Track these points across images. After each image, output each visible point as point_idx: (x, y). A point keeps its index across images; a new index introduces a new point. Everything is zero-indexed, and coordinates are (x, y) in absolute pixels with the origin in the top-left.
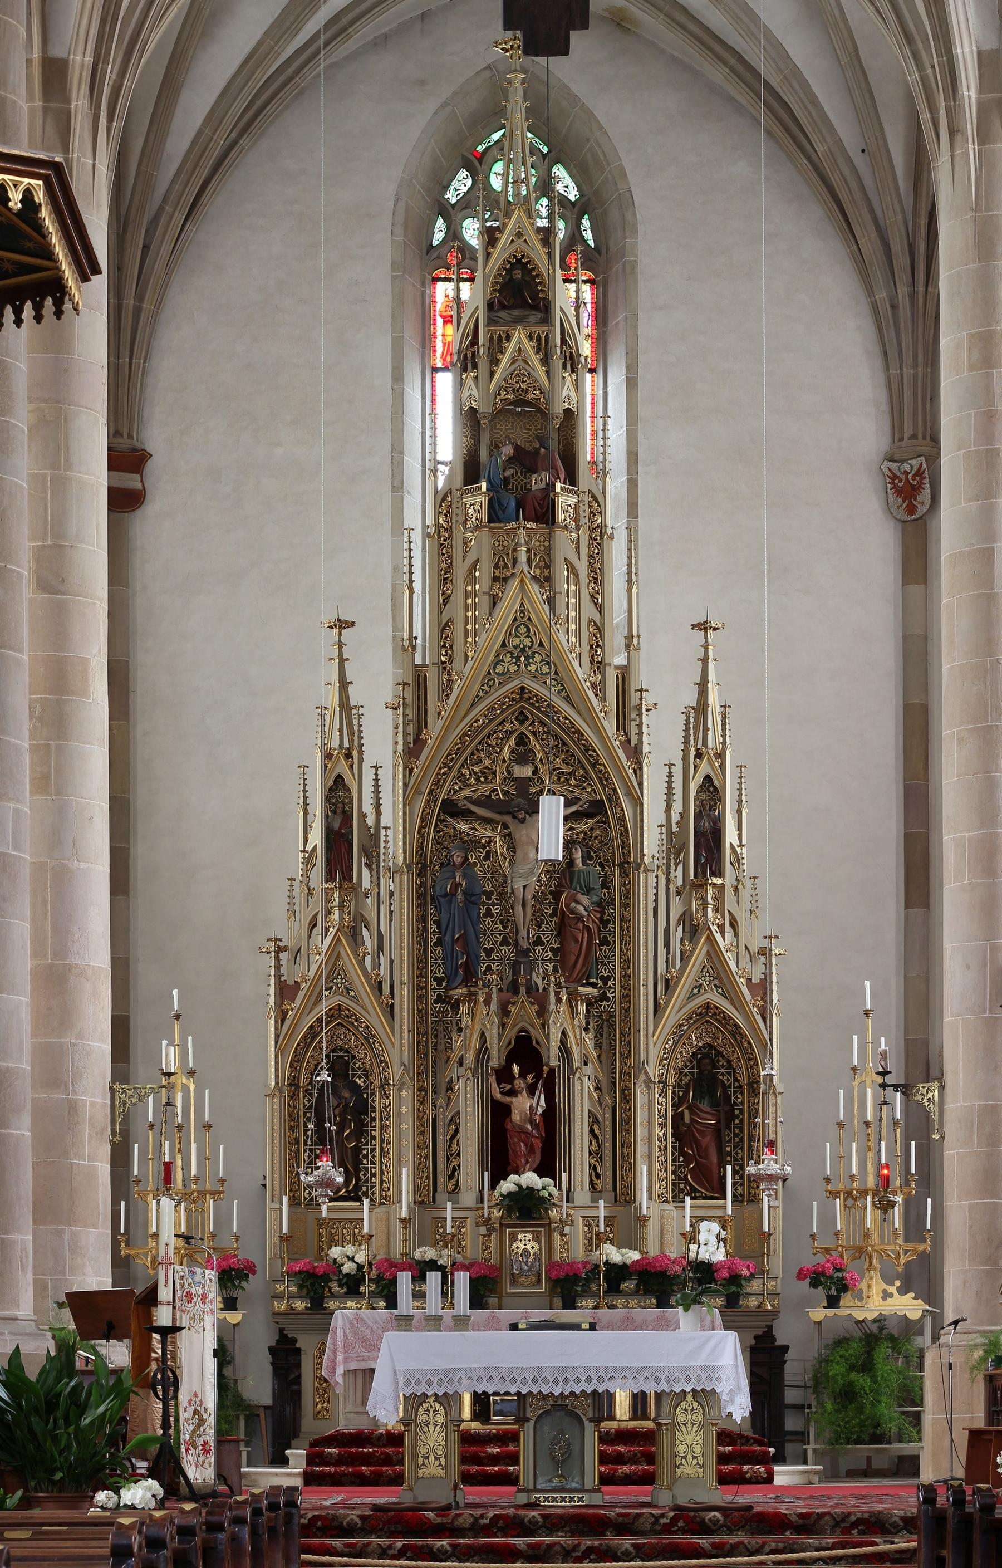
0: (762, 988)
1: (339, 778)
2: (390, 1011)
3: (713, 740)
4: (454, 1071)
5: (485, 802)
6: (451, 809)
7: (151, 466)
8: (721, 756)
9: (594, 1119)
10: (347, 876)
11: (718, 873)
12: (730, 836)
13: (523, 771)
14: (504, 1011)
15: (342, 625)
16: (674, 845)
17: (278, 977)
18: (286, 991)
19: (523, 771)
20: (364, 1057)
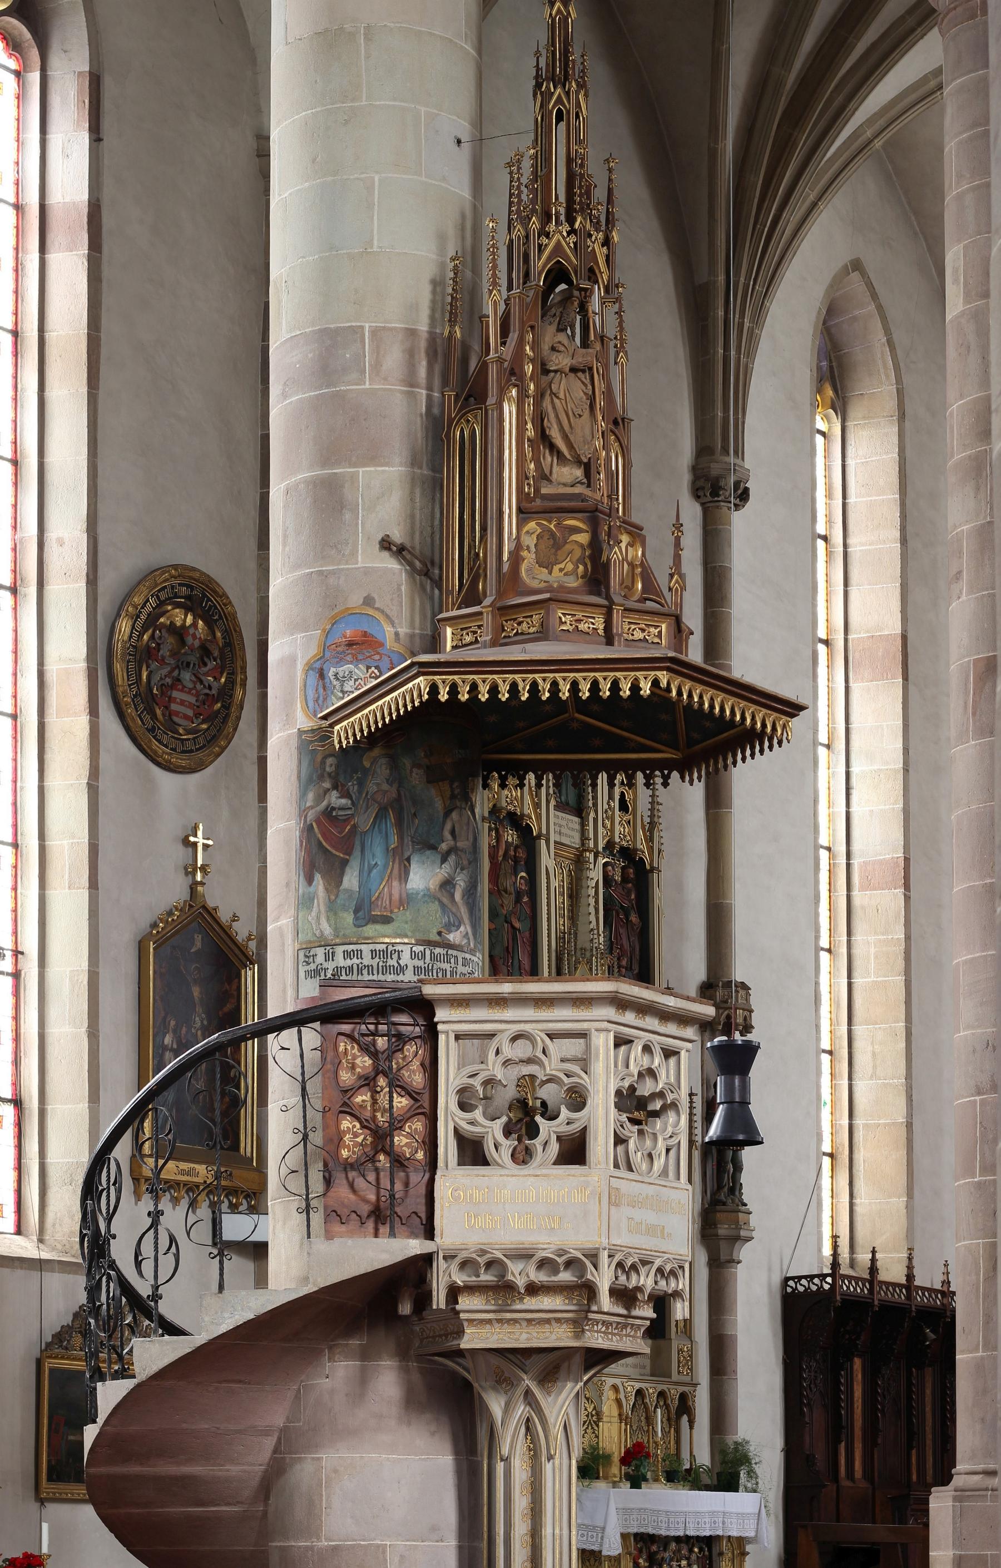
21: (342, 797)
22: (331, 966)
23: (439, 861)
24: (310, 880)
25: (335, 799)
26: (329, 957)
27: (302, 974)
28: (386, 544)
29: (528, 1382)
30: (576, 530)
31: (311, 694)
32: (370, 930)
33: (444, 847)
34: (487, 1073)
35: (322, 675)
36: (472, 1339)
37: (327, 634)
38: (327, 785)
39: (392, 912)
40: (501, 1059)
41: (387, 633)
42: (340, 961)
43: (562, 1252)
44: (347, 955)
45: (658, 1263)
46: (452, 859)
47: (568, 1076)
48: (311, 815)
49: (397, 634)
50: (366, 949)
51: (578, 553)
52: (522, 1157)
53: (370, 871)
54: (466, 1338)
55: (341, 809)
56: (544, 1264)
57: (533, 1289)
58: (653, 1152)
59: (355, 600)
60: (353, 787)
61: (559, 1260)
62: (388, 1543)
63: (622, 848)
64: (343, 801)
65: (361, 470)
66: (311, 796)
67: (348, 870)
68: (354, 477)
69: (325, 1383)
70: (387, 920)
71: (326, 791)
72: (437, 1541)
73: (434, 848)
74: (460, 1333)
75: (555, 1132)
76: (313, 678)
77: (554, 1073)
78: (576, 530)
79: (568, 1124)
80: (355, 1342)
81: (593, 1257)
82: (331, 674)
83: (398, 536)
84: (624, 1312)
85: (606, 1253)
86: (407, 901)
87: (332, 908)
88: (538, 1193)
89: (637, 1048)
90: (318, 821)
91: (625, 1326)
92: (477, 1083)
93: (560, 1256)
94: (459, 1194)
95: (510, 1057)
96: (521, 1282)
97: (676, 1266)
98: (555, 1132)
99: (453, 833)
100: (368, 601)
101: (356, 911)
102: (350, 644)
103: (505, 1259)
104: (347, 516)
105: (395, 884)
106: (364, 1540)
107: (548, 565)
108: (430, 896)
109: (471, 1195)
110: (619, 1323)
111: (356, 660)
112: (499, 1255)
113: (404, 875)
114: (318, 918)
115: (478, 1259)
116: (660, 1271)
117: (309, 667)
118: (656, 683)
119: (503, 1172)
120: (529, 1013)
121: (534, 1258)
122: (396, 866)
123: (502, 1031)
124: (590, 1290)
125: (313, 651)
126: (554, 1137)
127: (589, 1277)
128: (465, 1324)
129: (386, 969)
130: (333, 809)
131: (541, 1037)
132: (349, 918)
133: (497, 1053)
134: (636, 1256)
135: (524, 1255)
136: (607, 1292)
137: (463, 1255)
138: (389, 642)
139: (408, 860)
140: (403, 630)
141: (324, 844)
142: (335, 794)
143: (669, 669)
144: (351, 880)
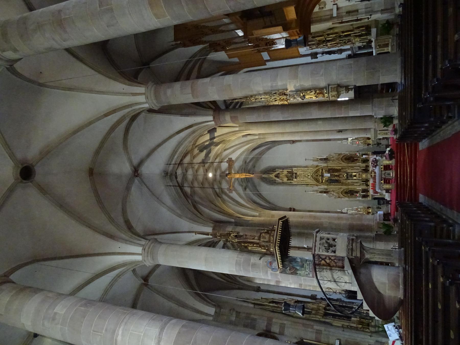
0: (339, 154)
1: (319, 192)
2: (341, 188)
3: (316, 159)
4: (347, 182)
5: (321, 179)
6: (322, 182)
7: (291, 207)
8: (317, 158)
9: (352, 169)
10: (328, 192)
11: (328, 158)
12: (325, 157)
13: (319, 176)
14: (341, 178)
15: (305, 192)
16: (326, 162)
17: (338, 198)
18: (339, 197)
19: (319, 176)
20: (345, 191)
22: (309, 272)
24: (297, 273)
25: (288, 269)
26: (307, 272)
27: (309, 276)
28: (260, 259)
31: (275, 270)
32: (305, 266)
35: (273, 269)
36: (359, 255)
37: (269, 267)
41: (270, 260)
42: (308, 270)
43: (347, 242)
44: (307, 269)
49: (270, 259)
50: (307, 267)
51: (265, 235)
52: (335, 246)
56: (349, 244)
57: (352, 245)
59: (265, 263)
60: (287, 266)
64: (289, 268)
68: (252, 262)
74: (358, 257)
76: (273, 270)
81: (348, 238)
82: (273, 267)
83: (259, 258)
87: (301, 271)
96: (351, 247)
100: (266, 262)
102: (270, 265)
104: (256, 263)
107: (265, 238)
111: (272, 264)
113: (298, 262)
117: (272, 270)
118: (281, 222)
120: (317, 243)
124: (353, 240)
125: (270, 270)
129: (309, 265)
132: (303, 269)
135: (348, 246)
137: (347, 253)
138: (271, 260)
140: (270, 259)
144: (298, 268)
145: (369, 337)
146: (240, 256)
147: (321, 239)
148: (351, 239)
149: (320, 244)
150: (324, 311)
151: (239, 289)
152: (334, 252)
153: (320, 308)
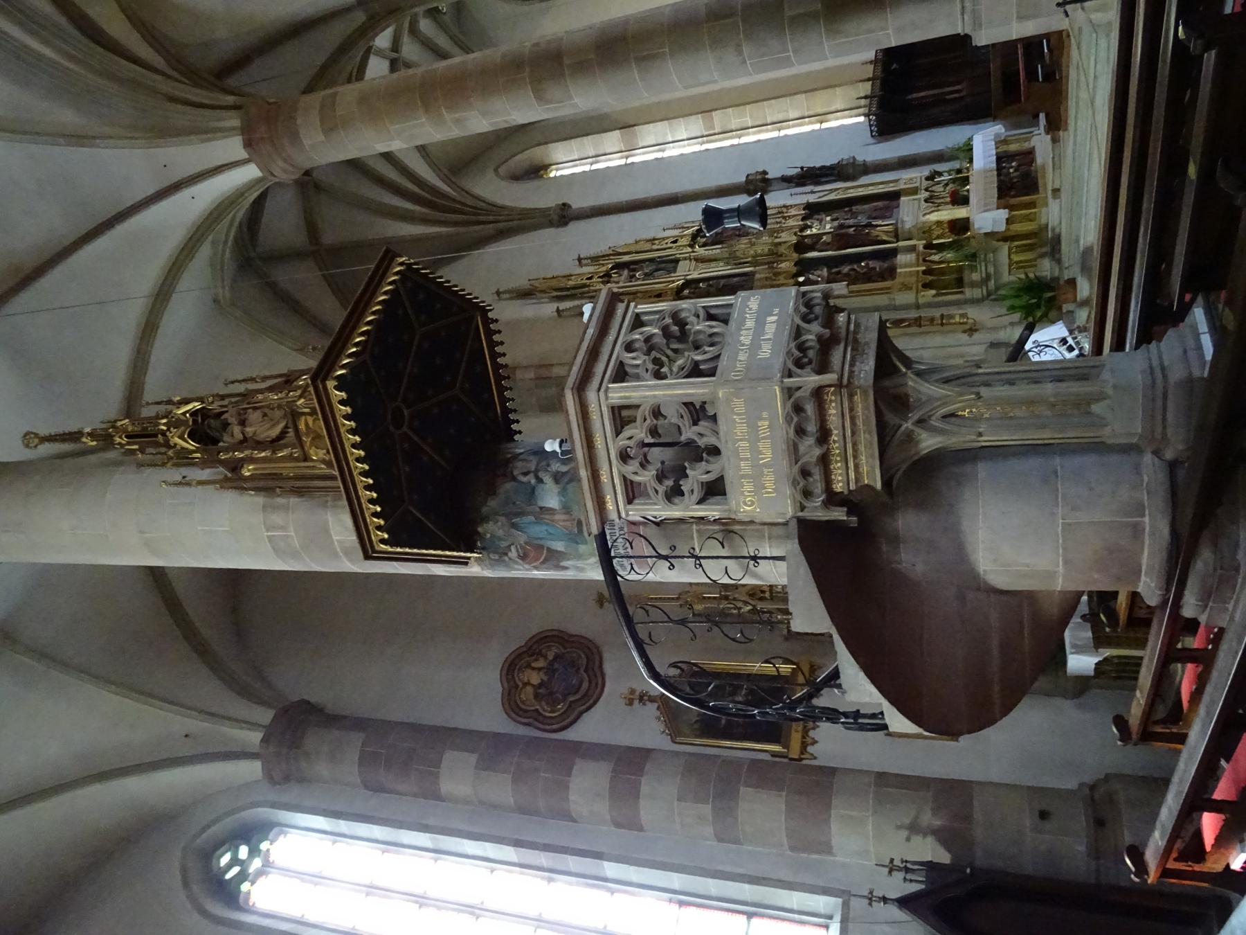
21: (511, 550)
23: (542, 485)
25: (513, 553)
29: (908, 425)
30: (307, 424)
33: (533, 481)
34: (652, 481)
38: (506, 558)
39: (574, 520)
40: (640, 471)
43: (788, 420)
45: (798, 321)
46: (541, 474)
47: (645, 420)
48: (527, 566)
53: (551, 534)
54: (872, 483)
55: (518, 551)
56: (800, 432)
58: (708, 333)
60: (504, 544)
61: (795, 419)
62: (1061, 521)
63: (692, 240)
65: (335, 538)
66: (516, 566)
67: (553, 548)
69: (920, 568)
70: (579, 523)
71: (510, 559)
72: (1057, 476)
73: (533, 489)
75: (690, 427)
77: (644, 431)
78: (307, 424)
79: (682, 417)
80: (885, 548)
81: (789, 392)
84: (842, 345)
85: (786, 380)
86: (567, 509)
88: (741, 440)
89: (627, 357)
90: (530, 564)
91: (856, 340)
92: (661, 489)
93: (792, 419)
94: (749, 501)
95: (638, 464)
96: (817, 452)
97: (801, 301)
98: (690, 427)
99: (526, 474)
101: (577, 543)
103: (800, 463)
105: (557, 517)
106: (1058, 541)
108: (563, 492)
109: (749, 492)
110: (853, 349)
112: (796, 469)
114: (587, 564)
115: (801, 485)
116: (805, 319)
119: (726, 465)
121: (796, 441)
122: (547, 517)
123: (619, 472)
124: (818, 393)
126: (695, 428)
127: (808, 394)
128: (859, 484)
130: (519, 556)
131: (622, 442)
133: (636, 473)
134: (791, 346)
136: (821, 377)
137: (799, 497)
139: (541, 508)
141: (541, 560)
142: (510, 554)
143: (324, 381)
144: (559, 546)
145: (965, 337)
146: (277, 518)
147: (621, 417)
148: (804, 393)
149: (624, 457)
150: (795, 256)
151: (501, 235)
152: (714, 489)
153: (782, 249)
